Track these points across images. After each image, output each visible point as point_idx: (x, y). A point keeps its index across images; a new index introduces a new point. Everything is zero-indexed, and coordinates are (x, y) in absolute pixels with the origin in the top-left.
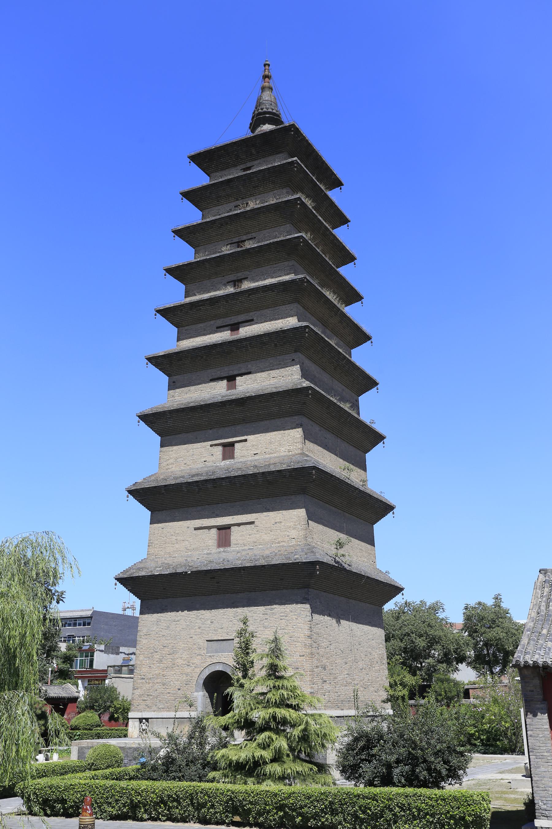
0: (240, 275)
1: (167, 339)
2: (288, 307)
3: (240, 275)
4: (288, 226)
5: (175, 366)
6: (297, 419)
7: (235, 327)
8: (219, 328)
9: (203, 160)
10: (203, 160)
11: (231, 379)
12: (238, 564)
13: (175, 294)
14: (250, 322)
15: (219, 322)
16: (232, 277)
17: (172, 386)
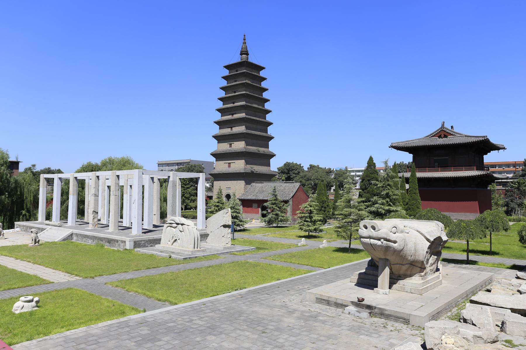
0: (234, 101)
1: (218, 117)
2: (243, 111)
3: (234, 101)
4: (244, 88)
5: (221, 124)
6: (244, 139)
7: (233, 115)
8: (229, 115)
9: (227, 67)
10: (227, 67)
11: (231, 128)
12: (231, 172)
13: (220, 105)
14: (236, 114)
15: (230, 113)
16: (232, 101)
17: (220, 129)
